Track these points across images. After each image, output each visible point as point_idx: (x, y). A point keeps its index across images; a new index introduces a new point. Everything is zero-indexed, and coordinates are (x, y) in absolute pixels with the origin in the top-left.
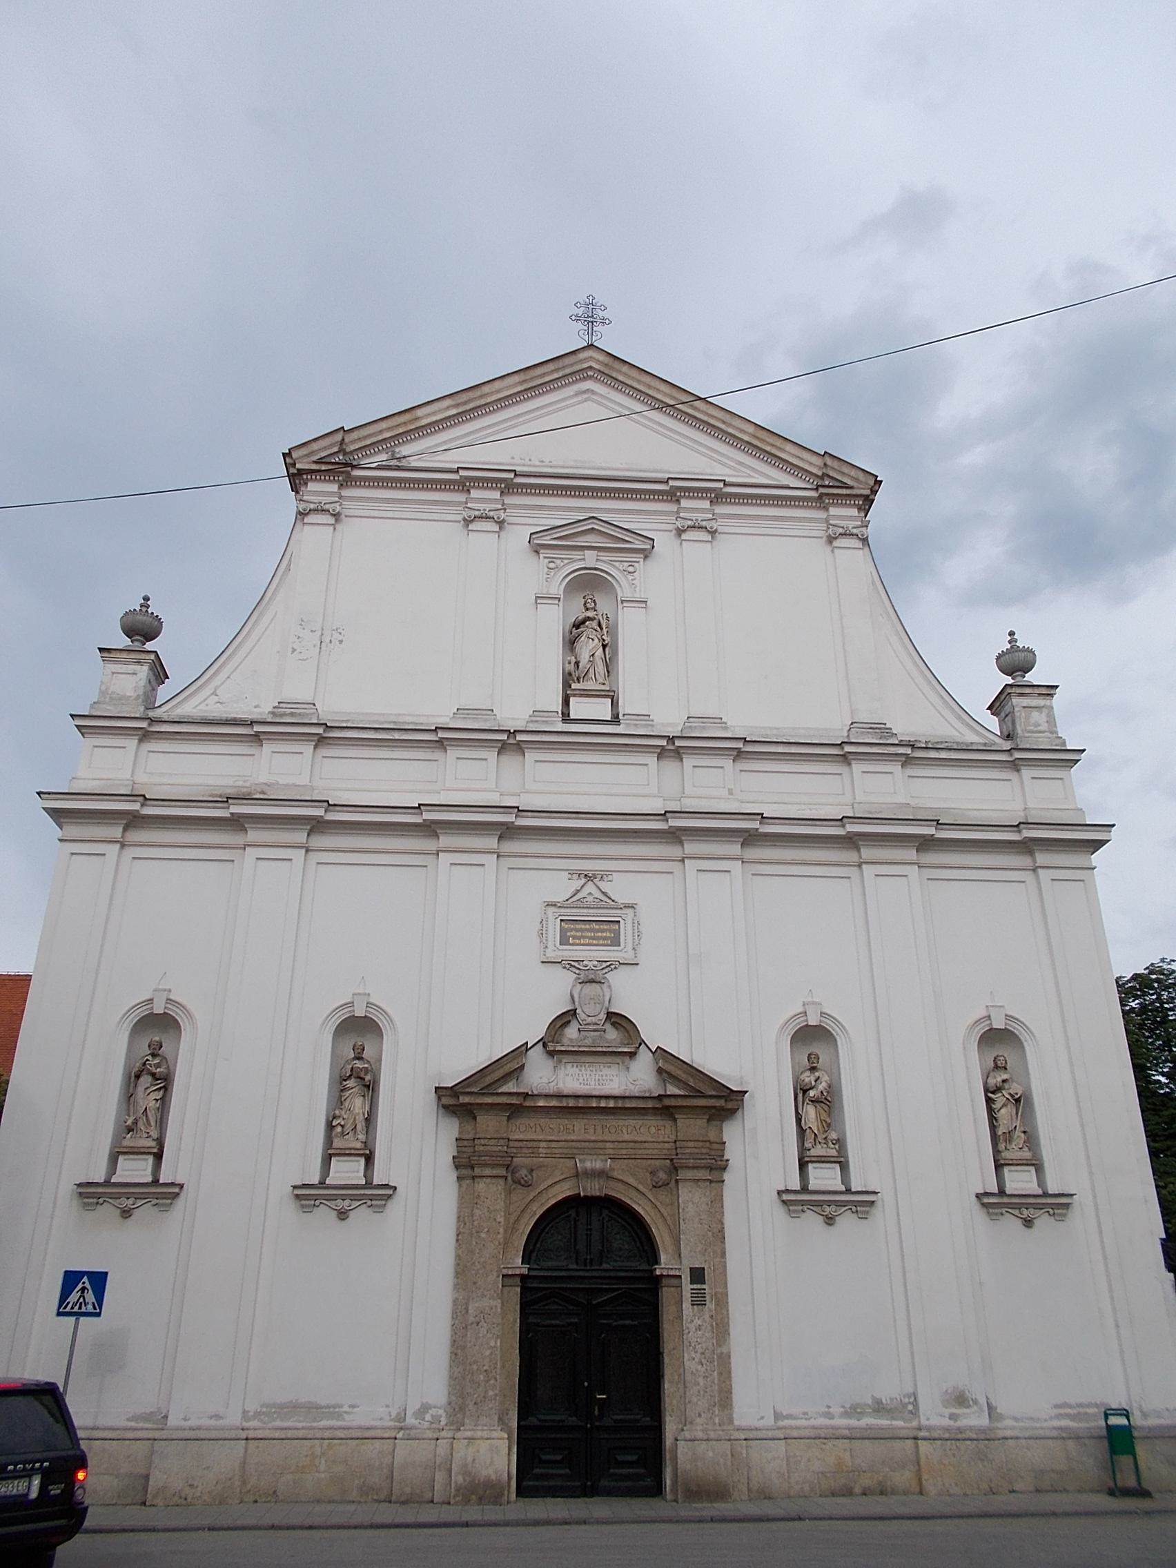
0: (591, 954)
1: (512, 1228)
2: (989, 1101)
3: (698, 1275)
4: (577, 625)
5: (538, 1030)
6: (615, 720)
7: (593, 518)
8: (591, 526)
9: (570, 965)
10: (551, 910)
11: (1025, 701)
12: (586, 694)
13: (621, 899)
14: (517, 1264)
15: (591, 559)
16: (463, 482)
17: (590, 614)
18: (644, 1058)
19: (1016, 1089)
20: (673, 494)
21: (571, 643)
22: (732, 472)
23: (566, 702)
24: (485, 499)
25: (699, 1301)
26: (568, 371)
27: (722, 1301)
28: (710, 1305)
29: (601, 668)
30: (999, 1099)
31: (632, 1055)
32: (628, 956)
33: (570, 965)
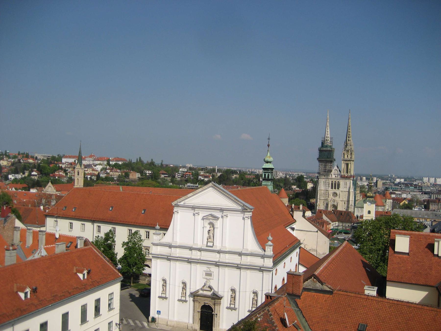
0: (208, 277)
1: (199, 307)
2: (253, 300)
3: (216, 314)
4: (209, 230)
5: (201, 287)
6: (212, 247)
7: (211, 214)
8: (212, 215)
9: (206, 279)
10: (204, 272)
11: (267, 247)
12: (210, 242)
13: (212, 271)
14: (200, 310)
15: (211, 221)
16: (193, 208)
17: (210, 229)
18: (213, 290)
19: (256, 299)
20: (222, 210)
21: (209, 233)
22: (232, 204)
23: (207, 242)
24: (197, 211)
25: (216, 317)
26: (208, 186)
27: (219, 317)
28: (218, 317)
29: (212, 237)
30: (254, 299)
31: (211, 291)
32: (212, 278)
33: (206, 279)
